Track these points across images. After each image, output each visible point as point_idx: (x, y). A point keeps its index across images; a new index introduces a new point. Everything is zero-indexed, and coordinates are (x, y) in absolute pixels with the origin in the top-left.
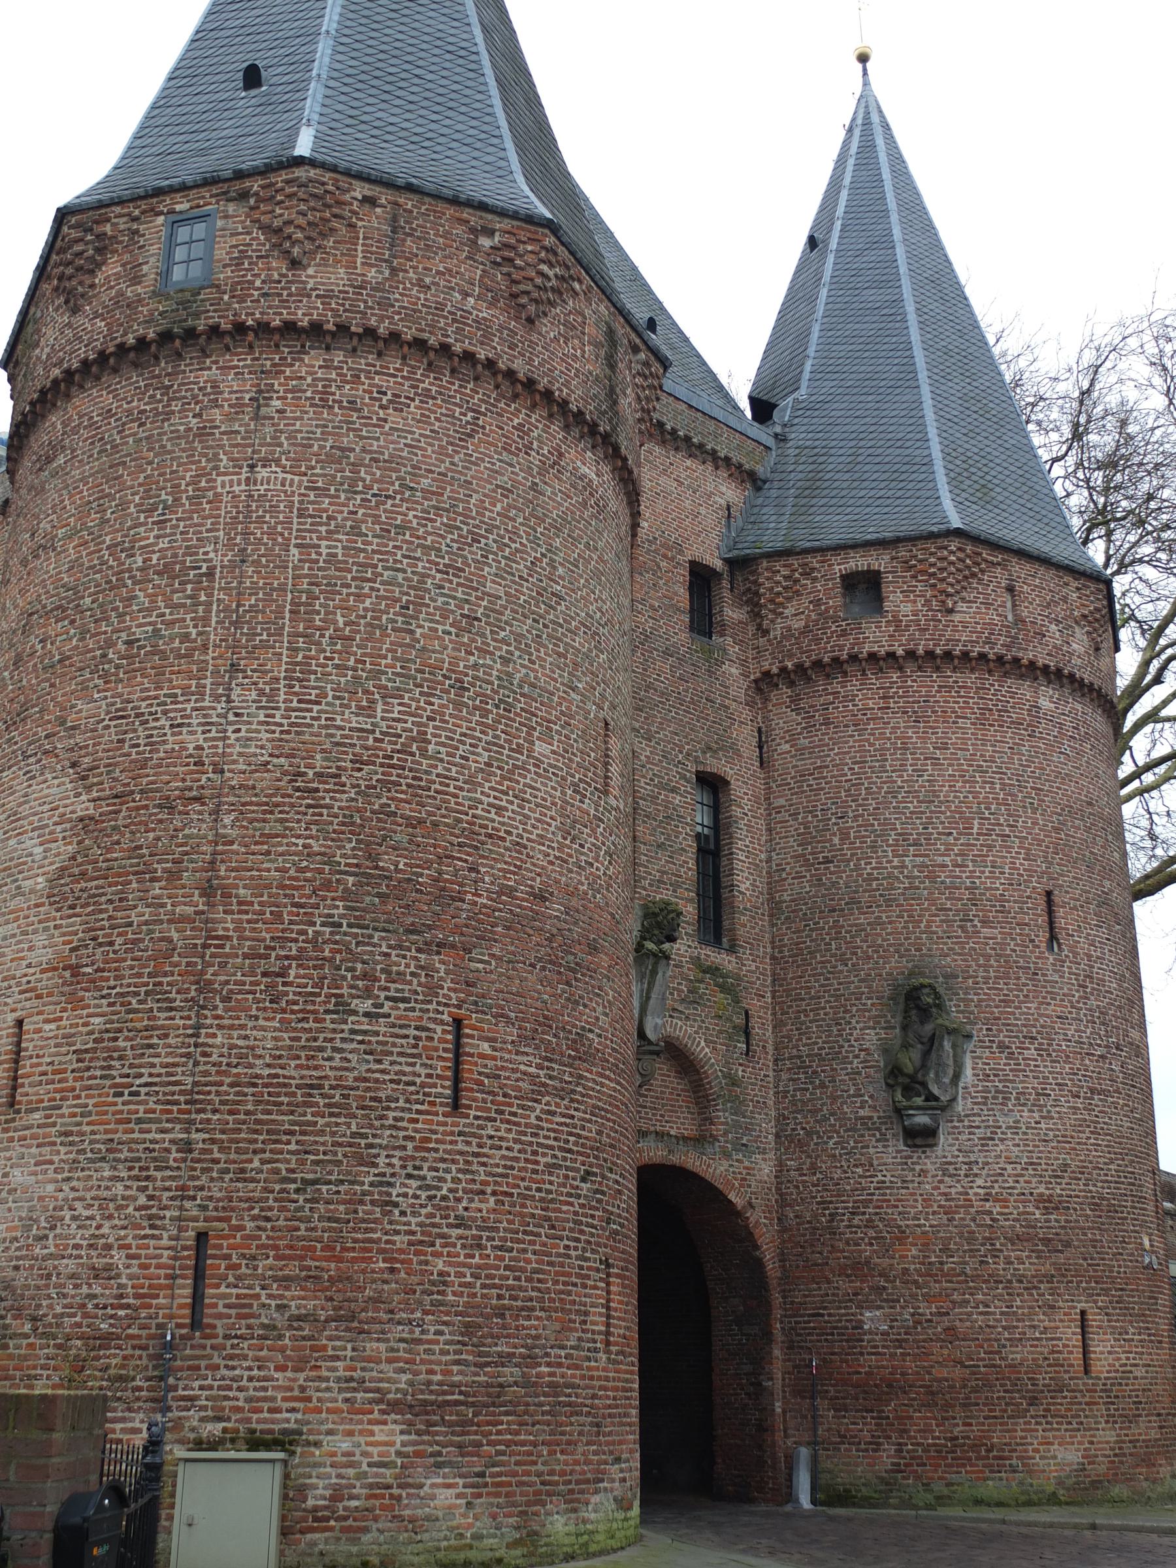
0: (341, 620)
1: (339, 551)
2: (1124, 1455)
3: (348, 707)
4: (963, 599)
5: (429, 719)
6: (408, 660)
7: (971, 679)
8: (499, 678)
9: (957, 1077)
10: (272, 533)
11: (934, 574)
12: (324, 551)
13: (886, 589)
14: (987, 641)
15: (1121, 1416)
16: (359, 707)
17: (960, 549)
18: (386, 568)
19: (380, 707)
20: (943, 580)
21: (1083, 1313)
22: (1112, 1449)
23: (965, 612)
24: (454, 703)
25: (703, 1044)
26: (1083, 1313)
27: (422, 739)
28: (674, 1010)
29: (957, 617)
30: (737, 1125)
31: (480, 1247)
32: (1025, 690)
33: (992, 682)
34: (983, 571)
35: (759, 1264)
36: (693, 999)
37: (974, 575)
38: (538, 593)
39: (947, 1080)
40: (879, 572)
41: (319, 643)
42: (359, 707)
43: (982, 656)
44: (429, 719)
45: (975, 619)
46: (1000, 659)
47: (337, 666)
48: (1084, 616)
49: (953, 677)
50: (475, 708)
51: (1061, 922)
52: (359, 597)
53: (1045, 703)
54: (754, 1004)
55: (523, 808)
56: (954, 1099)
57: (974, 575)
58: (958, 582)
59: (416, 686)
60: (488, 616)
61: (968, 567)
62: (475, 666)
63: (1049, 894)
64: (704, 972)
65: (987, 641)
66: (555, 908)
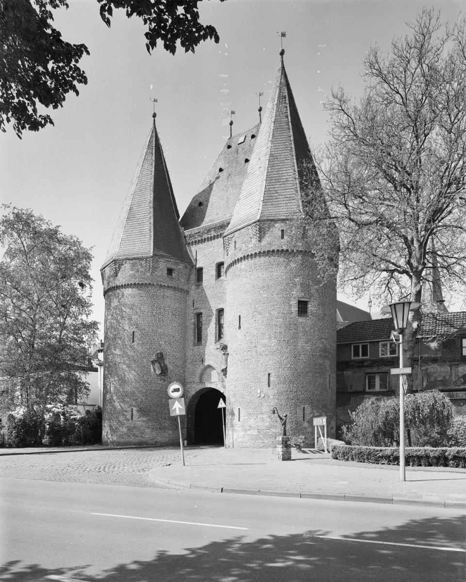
63: (240, 316)
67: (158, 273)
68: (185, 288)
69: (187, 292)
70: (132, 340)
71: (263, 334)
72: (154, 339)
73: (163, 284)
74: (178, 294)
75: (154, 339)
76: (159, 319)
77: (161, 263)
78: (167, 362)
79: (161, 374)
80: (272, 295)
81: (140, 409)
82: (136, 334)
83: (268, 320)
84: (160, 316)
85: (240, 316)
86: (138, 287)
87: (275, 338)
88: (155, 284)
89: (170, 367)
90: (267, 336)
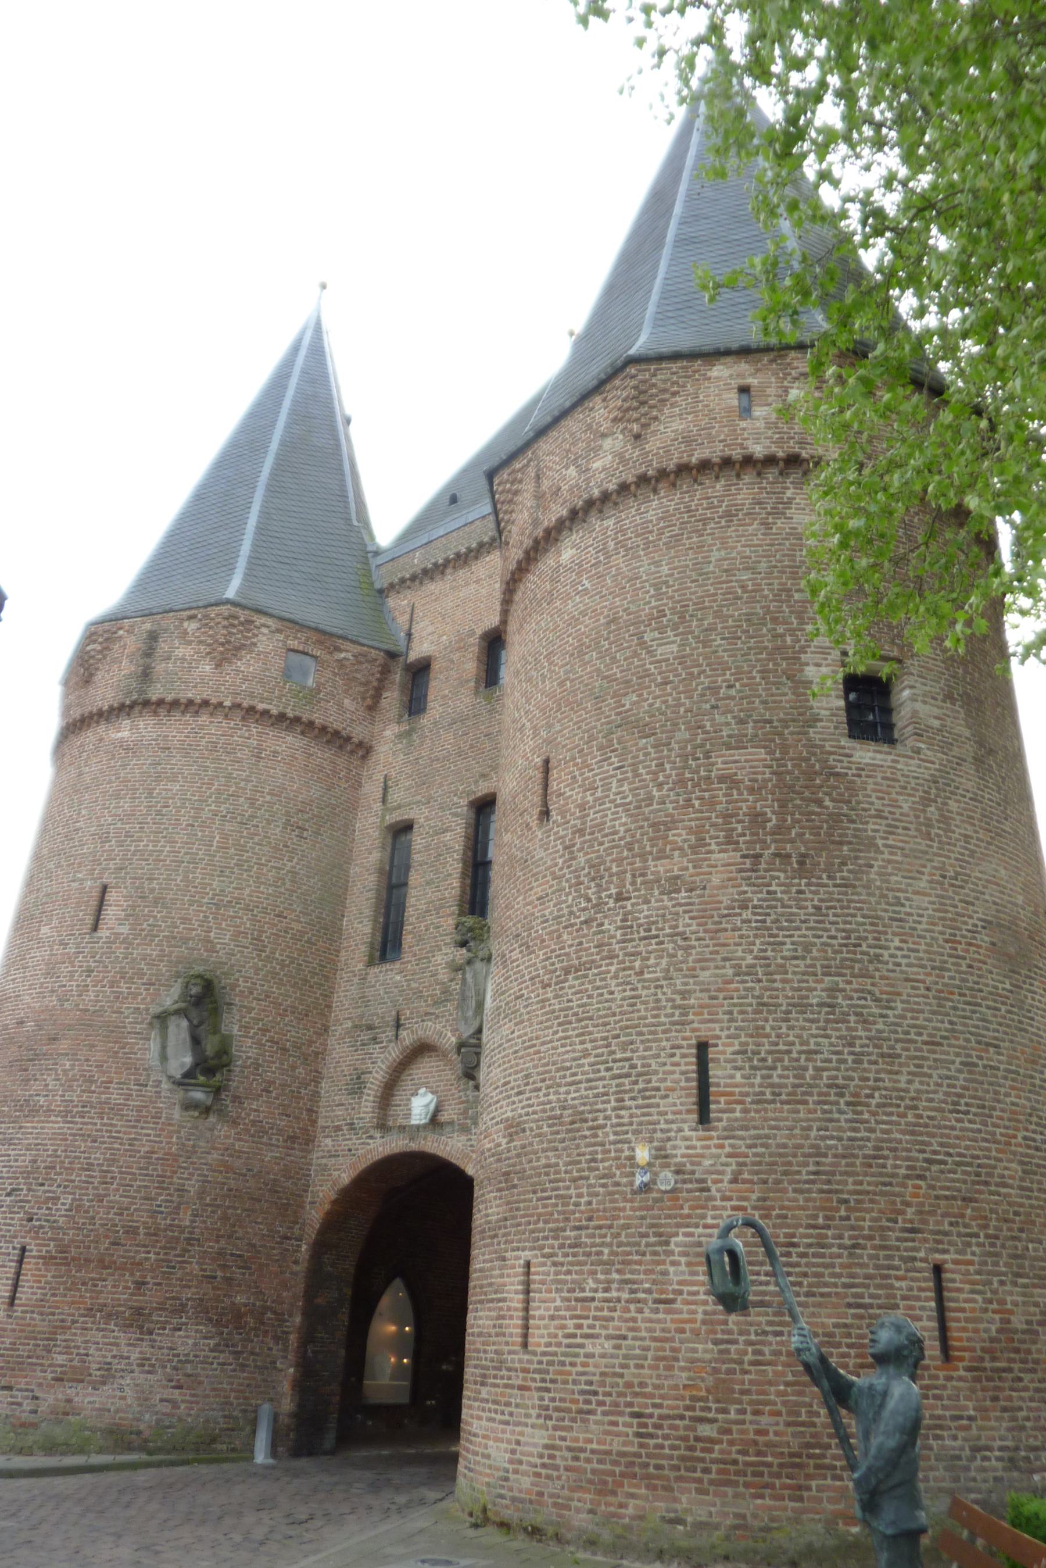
2: (556, 1468)
9: (480, 1005)
15: (557, 1409)
21: (528, 1265)
22: (541, 1456)
25: (449, 1034)
26: (528, 1265)
28: (427, 1014)
39: (470, 1013)
51: (554, 786)
56: (480, 1031)
63: (547, 762)
66: (30, 1025)
67: (247, 665)
68: (358, 732)
69: (365, 750)
70: (89, 920)
71: (661, 828)
72: (185, 920)
73: (261, 707)
74: (323, 755)
75: (185, 920)
76: (225, 837)
77: (265, 630)
78: (232, 1025)
79: (189, 1074)
80: (706, 643)
81: (63, 1249)
82: (112, 896)
83: (684, 757)
84: (228, 827)
85: (547, 762)
86: (155, 713)
87: (730, 841)
88: (227, 703)
89: (245, 1049)
90: (679, 836)
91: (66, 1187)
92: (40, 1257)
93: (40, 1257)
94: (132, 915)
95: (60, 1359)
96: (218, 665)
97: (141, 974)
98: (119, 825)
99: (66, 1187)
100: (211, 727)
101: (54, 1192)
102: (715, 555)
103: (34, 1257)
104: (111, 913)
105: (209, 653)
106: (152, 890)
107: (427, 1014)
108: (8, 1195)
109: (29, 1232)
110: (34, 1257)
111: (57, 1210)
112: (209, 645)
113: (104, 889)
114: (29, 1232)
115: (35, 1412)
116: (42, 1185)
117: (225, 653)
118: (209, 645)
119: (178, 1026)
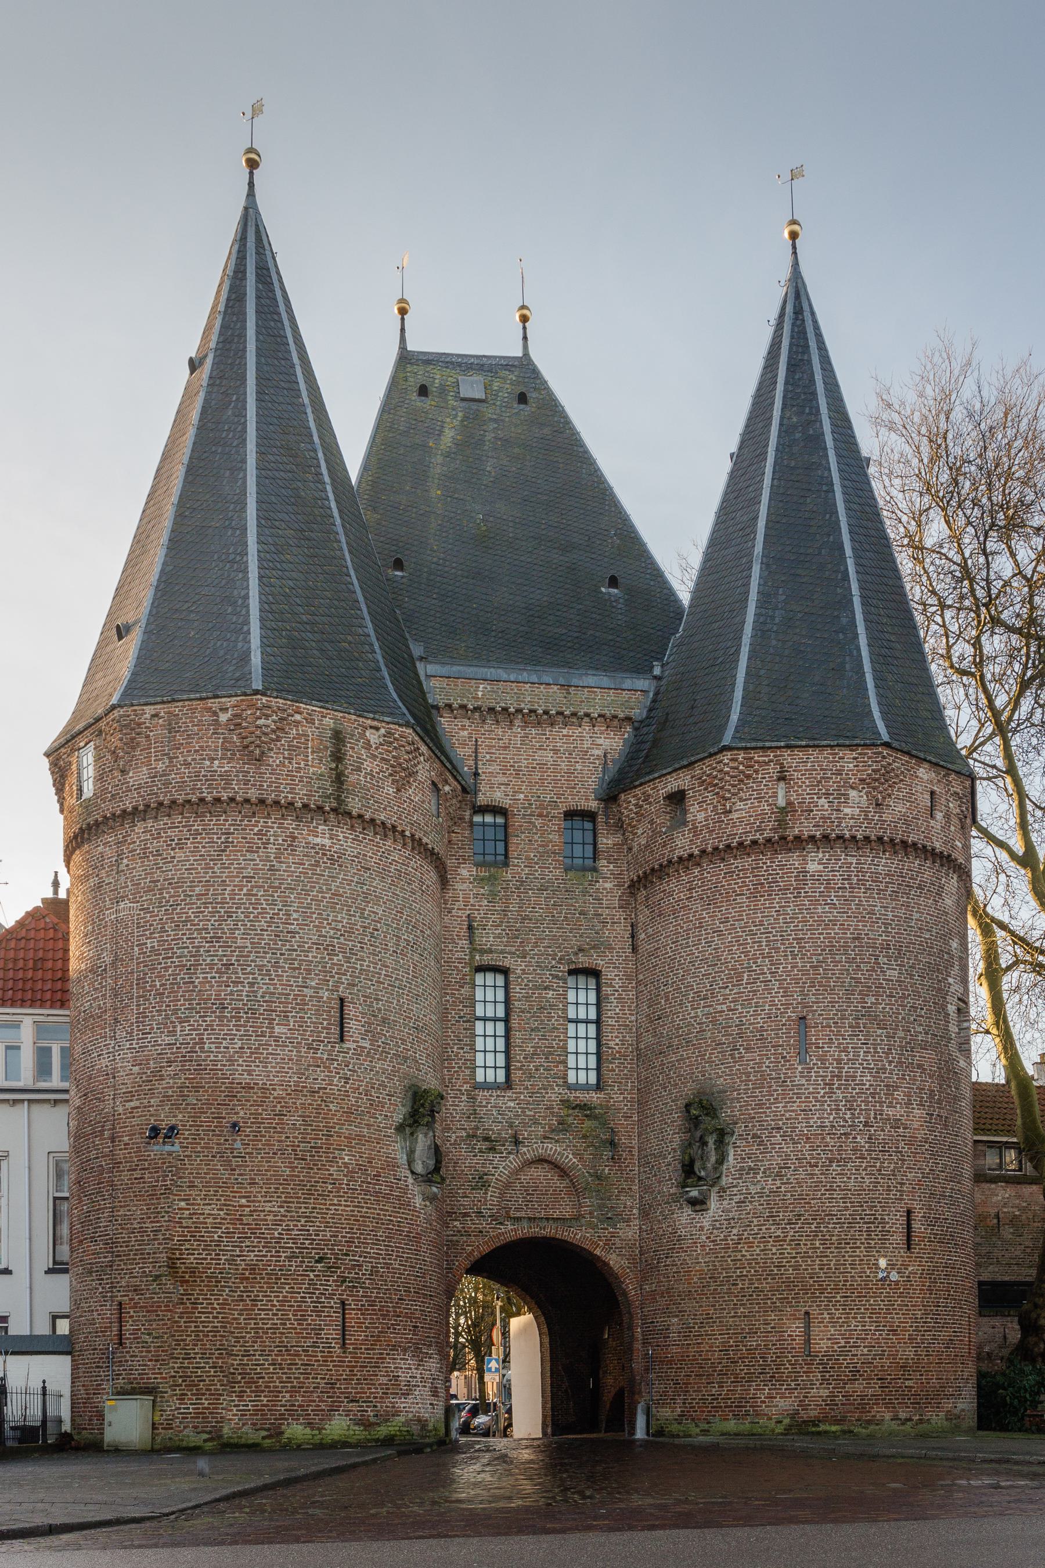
0: (158, 984)
1: (156, 944)
3: (163, 1032)
4: (741, 800)
5: (205, 1030)
6: (192, 1000)
7: (748, 862)
8: (247, 996)
10: (126, 941)
11: (717, 784)
12: (149, 945)
13: (689, 802)
14: (760, 829)
16: (169, 1032)
17: (731, 760)
18: (178, 948)
19: (179, 1029)
20: (722, 788)
23: (741, 810)
24: (218, 1017)
25: (571, 1156)
27: (201, 1042)
29: (735, 816)
30: (601, 1207)
31: (242, 1300)
32: (794, 860)
33: (765, 861)
34: (756, 772)
35: (625, 1294)
36: (563, 1126)
37: (748, 777)
38: (276, 936)
40: (684, 790)
41: (148, 1000)
42: (169, 1032)
43: (755, 842)
44: (205, 1030)
45: (748, 813)
46: (769, 840)
47: (157, 1011)
48: (862, 780)
49: (737, 863)
50: (232, 1017)
52: (166, 969)
53: (813, 867)
54: (620, 1123)
55: (267, 1067)
57: (748, 777)
58: (733, 786)
59: (197, 1013)
60: (238, 961)
61: (742, 772)
62: (231, 993)
64: (573, 1108)
65: (760, 829)
70: (335, 1030)
82: (350, 1010)
91: (365, 1257)
92: (358, 1309)
93: (358, 1309)
94: (368, 1032)
95: (384, 1380)
96: (399, 790)
97: (383, 1085)
98: (342, 940)
99: (365, 1257)
100: (397, 854)
101: (358, 1261)
102: (916, 916)
103: (353, 1309)
104: (353, 1026)
105: (391, 775)
106: (379, 1010)
107: (545, 1138)
108: (317, 1262)
109: (345, 1291)
110: (353, 1309)
111: (363, 1274)
112: (392, 766)
113: (342, 1000)
114: (345, 1291)
115: (377, 1416)
116: (347, 1255)
117: (402, 777)
118: (392, 766)
119: (426, 1135)
